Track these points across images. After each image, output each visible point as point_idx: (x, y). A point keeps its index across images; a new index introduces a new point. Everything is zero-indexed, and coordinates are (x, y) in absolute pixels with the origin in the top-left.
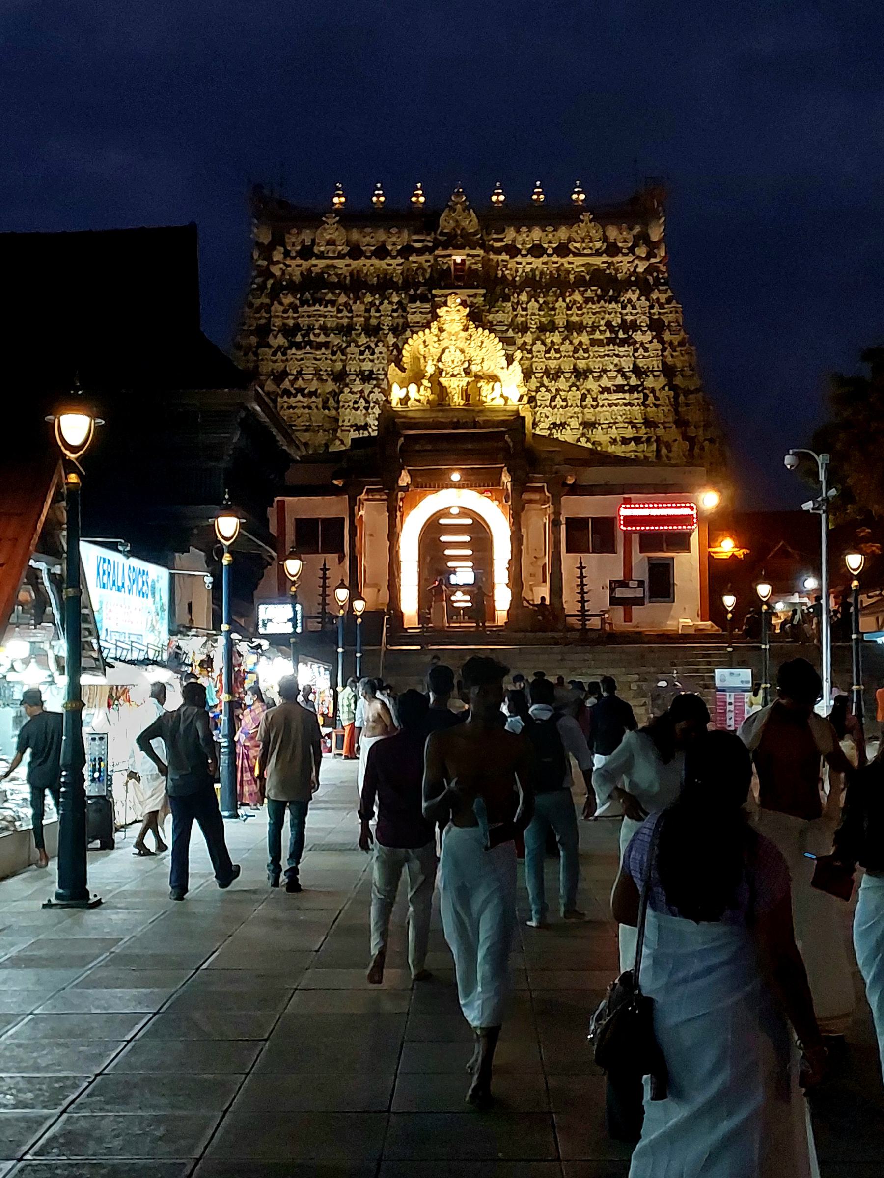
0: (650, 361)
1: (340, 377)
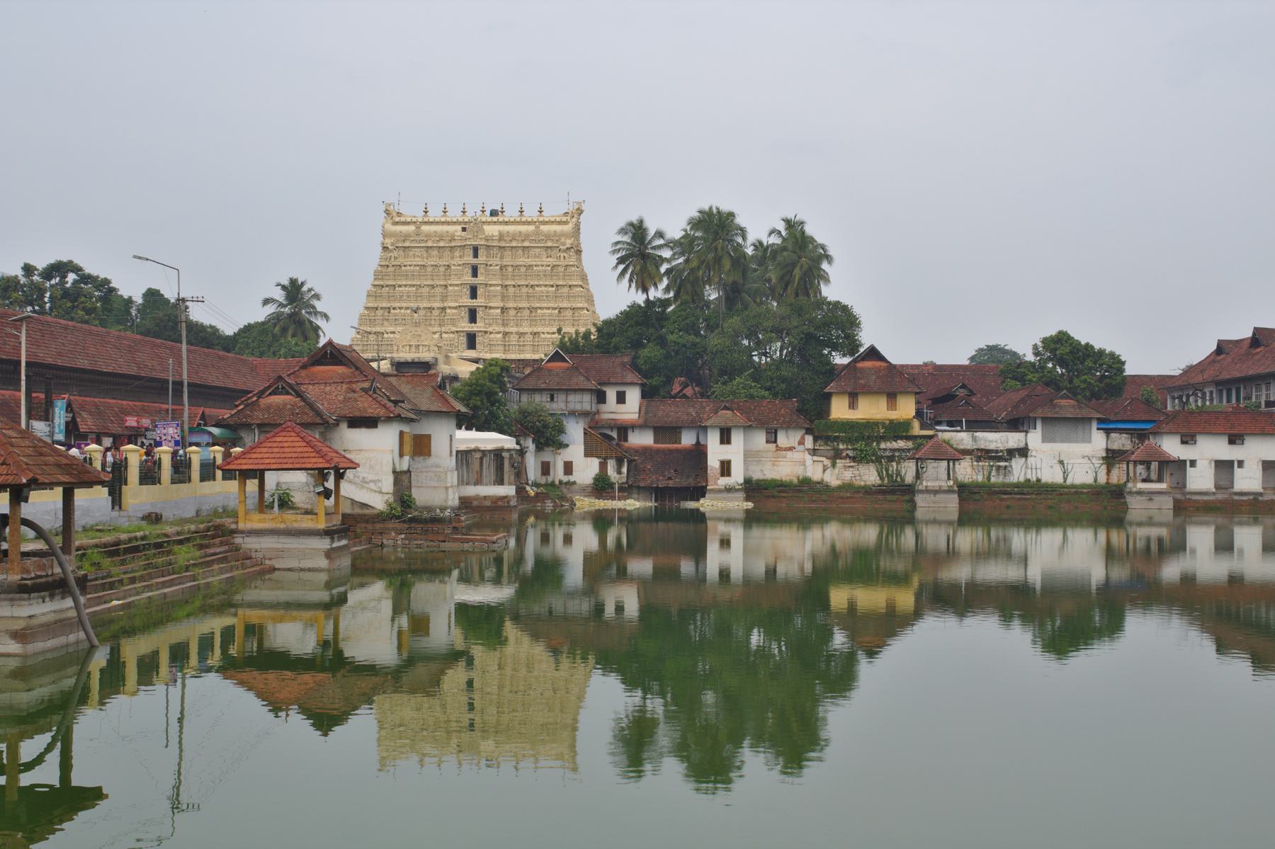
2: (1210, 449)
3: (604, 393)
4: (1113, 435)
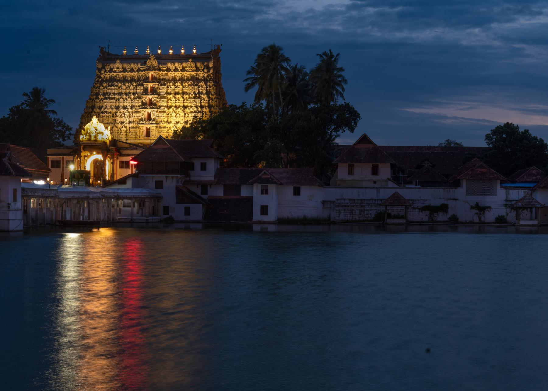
0: (205, 103)
1: (117, 108)
3: (193, 164)
4: (511, 191)
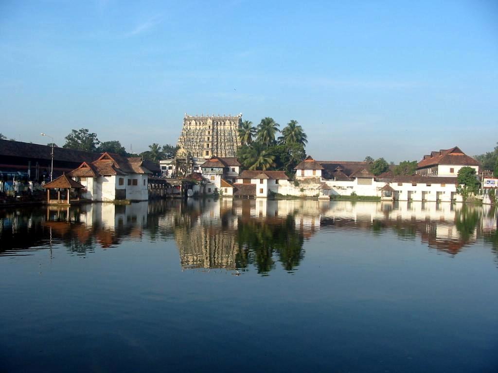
2: (407, 187)
